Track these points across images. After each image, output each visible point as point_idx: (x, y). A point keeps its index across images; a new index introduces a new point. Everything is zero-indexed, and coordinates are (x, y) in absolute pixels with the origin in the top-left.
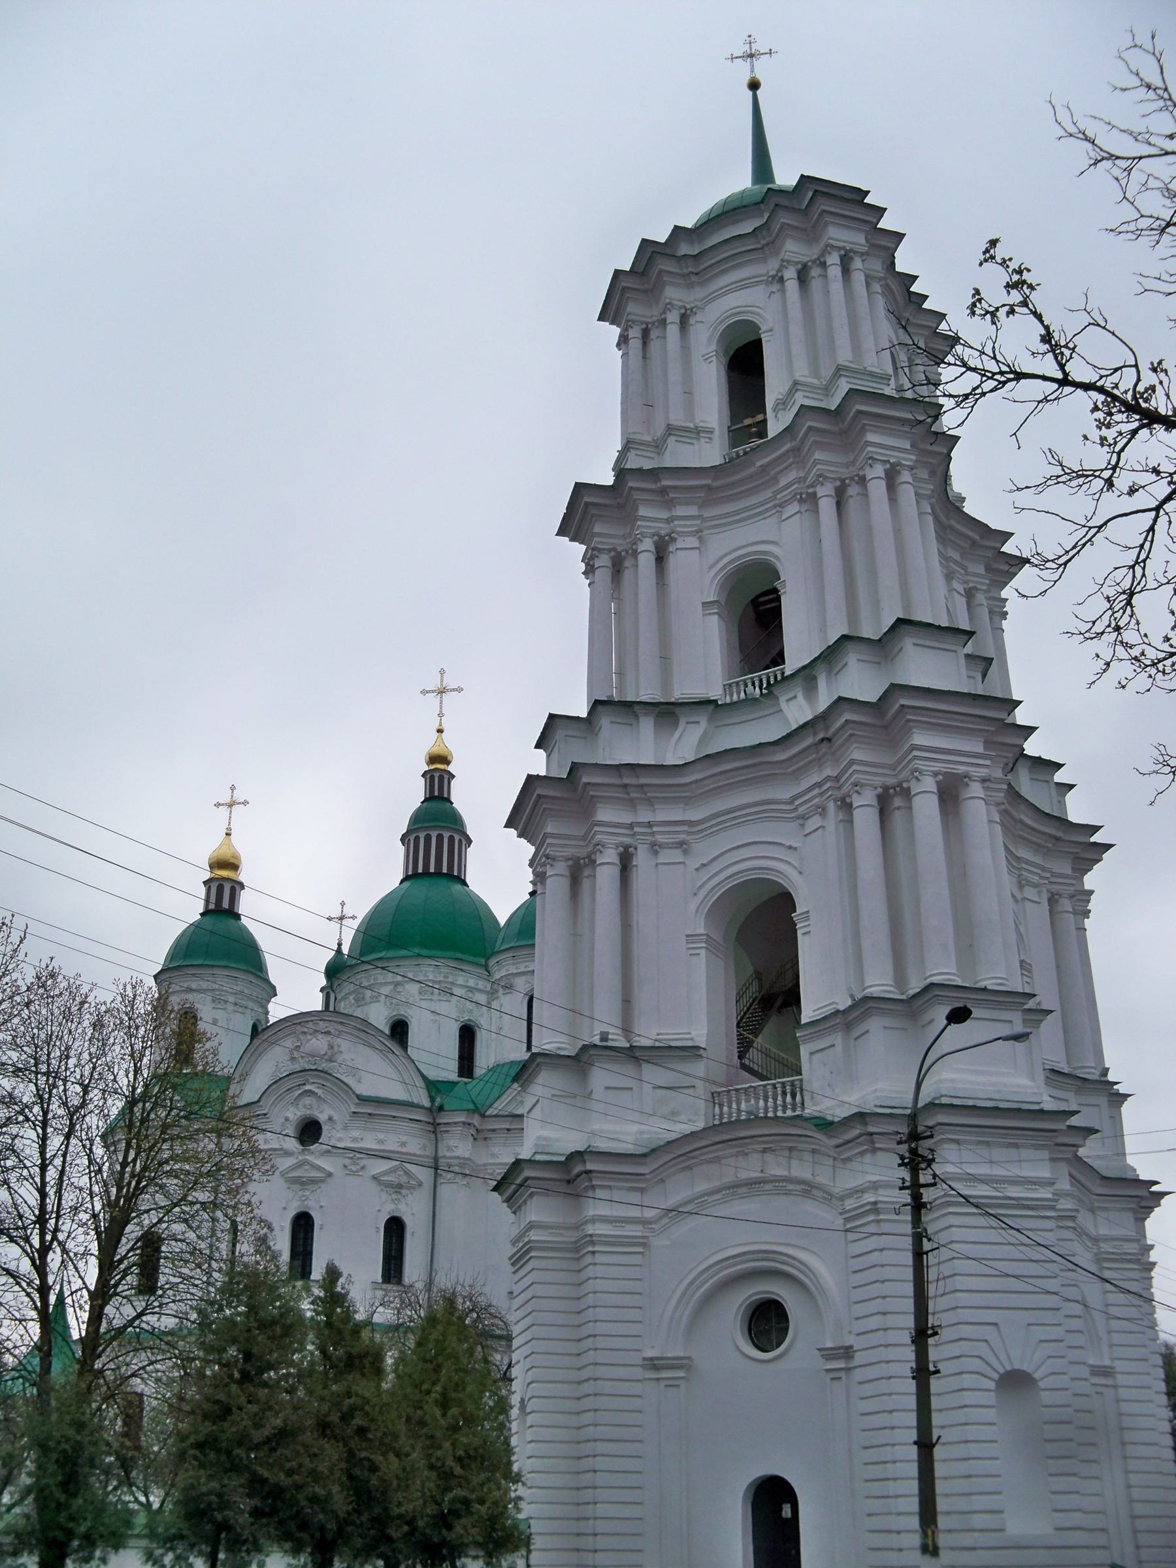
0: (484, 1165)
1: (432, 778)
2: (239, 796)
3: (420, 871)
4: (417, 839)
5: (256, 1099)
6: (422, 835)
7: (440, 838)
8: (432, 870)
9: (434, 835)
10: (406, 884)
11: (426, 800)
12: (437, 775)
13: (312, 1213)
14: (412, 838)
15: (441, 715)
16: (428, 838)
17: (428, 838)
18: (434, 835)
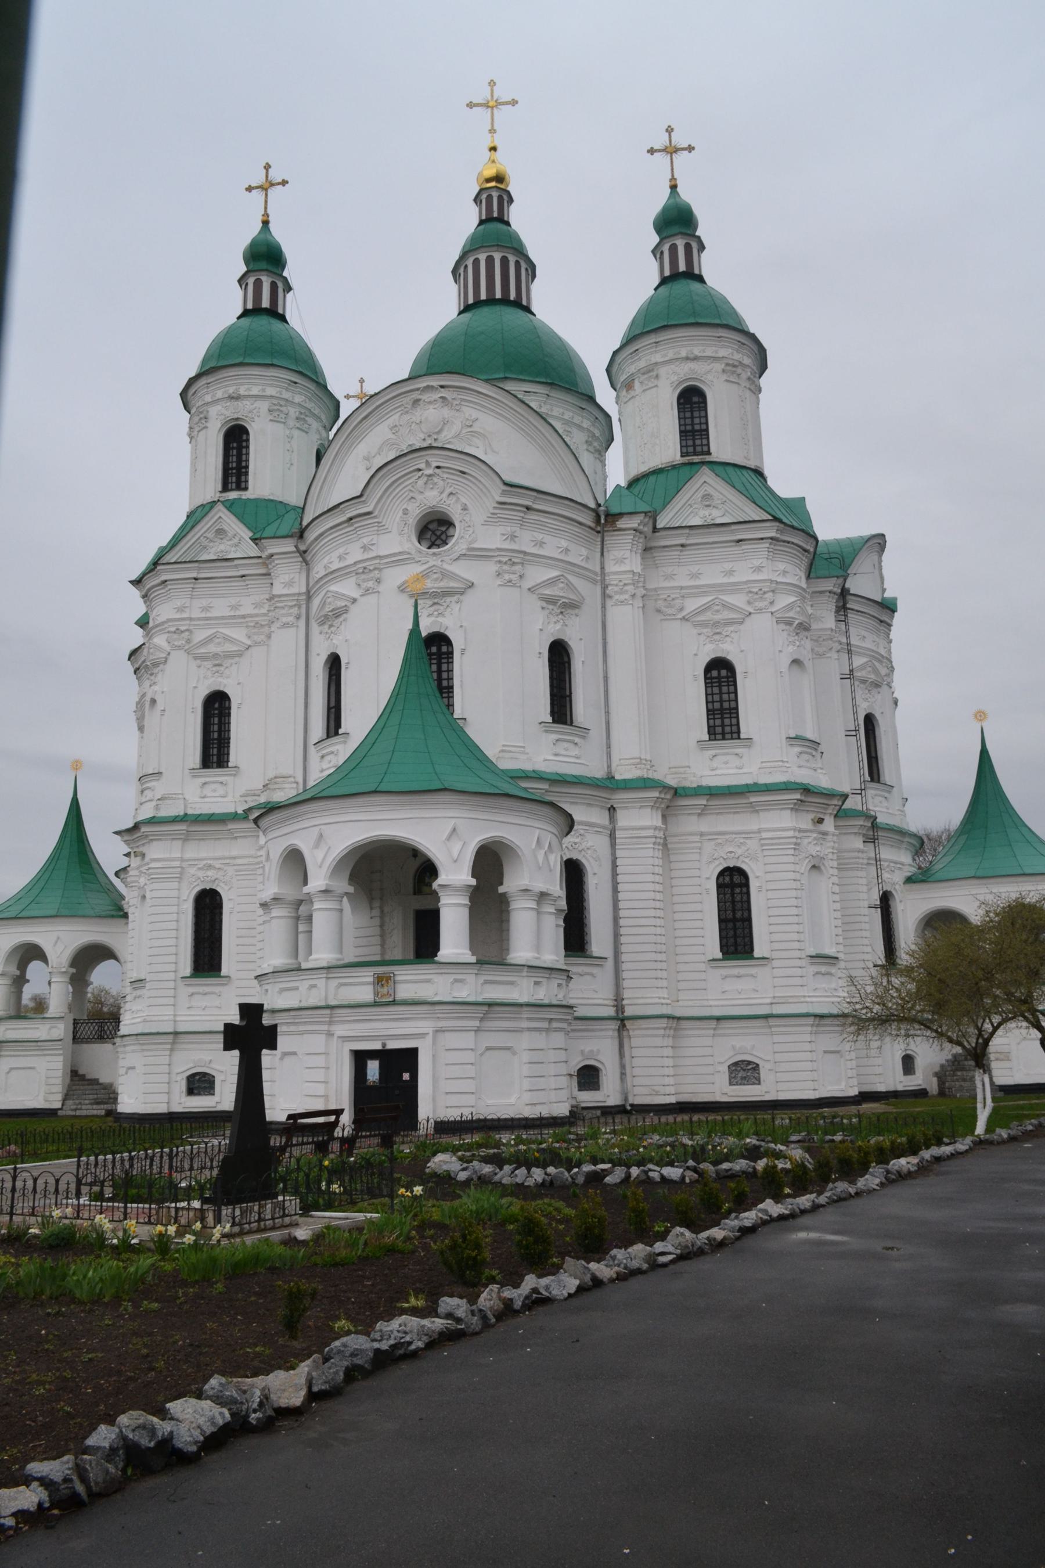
0: (655, 590)
1: (489, 198)
2: (276, 175)
3: (483, 297)
4: (476, 262)
5: (358, 494)
6: (482, 257)
7: (505, 261)
8: (498, 295)
9: (497, 256)
10: (467, 316)
11: (481, 222)
12: (495, 195)
13: (448, 633)
14: (470, 262)
15: (492, 131)
16: (490, 260)
17: (490, 260)
18: (497, 256)
